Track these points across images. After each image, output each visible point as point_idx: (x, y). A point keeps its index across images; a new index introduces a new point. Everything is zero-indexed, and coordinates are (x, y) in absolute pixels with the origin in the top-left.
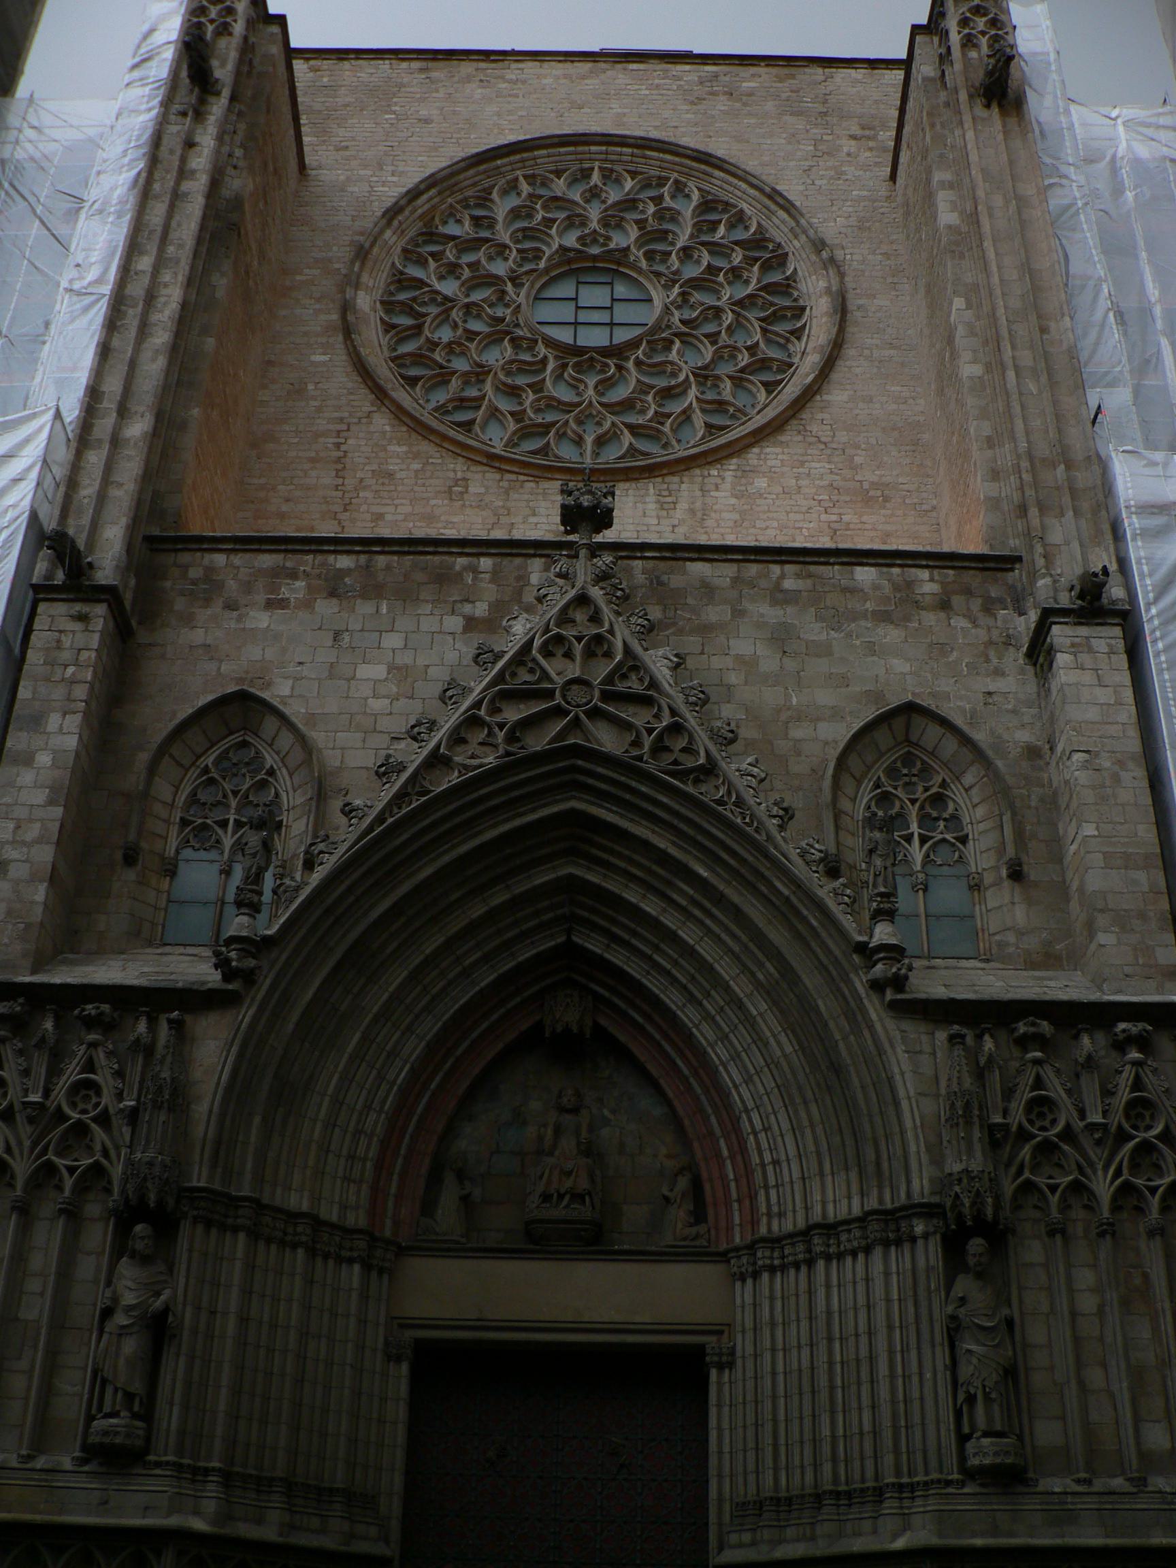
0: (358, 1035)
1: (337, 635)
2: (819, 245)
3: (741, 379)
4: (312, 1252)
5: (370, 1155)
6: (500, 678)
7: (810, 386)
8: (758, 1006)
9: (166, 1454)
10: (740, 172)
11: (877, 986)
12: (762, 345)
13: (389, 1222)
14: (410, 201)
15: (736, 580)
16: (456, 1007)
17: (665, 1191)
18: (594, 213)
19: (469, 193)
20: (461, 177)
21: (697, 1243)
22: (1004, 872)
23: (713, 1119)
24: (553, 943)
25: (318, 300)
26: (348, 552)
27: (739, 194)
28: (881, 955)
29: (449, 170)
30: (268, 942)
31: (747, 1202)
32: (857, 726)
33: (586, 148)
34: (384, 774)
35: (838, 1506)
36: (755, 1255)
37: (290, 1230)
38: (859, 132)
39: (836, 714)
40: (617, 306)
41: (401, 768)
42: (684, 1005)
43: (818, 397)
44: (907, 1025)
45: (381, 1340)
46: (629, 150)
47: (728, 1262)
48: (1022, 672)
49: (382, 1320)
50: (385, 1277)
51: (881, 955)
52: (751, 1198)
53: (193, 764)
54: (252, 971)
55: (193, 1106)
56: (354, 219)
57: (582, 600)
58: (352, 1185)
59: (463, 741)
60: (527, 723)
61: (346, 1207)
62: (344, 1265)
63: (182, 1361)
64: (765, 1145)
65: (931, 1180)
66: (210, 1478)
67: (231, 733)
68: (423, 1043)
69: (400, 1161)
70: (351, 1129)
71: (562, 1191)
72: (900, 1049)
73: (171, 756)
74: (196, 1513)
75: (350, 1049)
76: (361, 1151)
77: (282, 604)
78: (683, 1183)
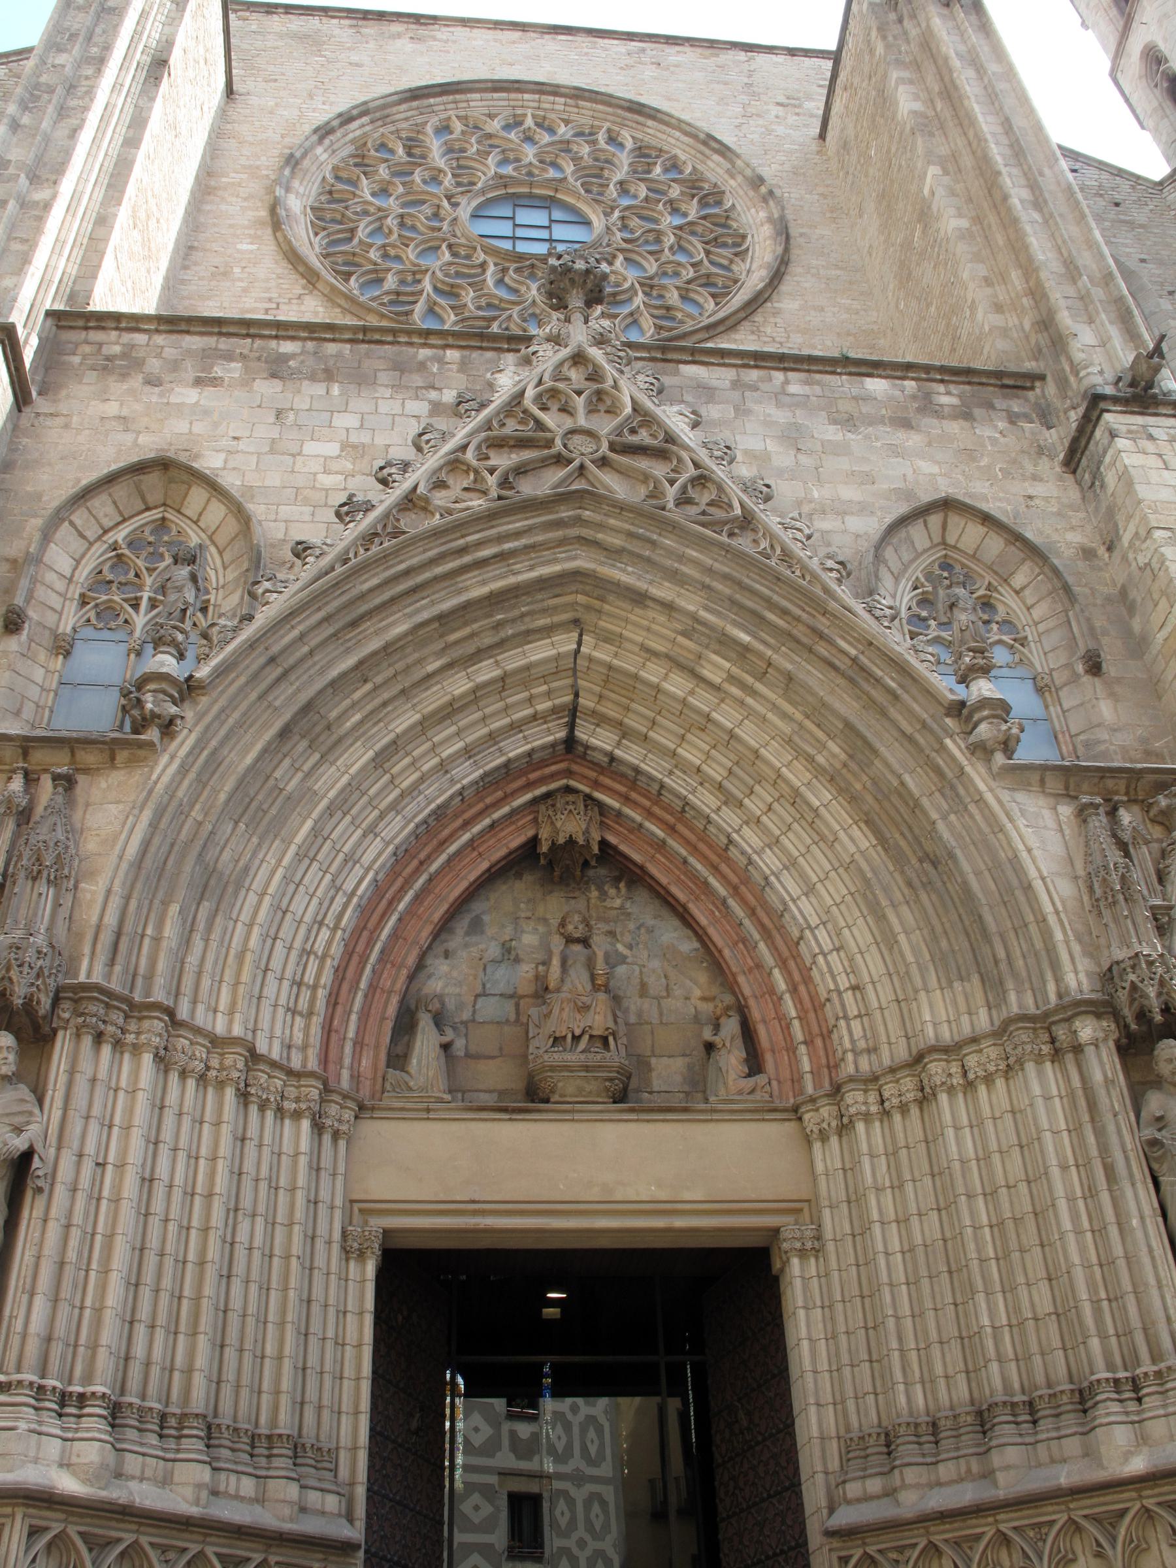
0: (309, 824)
1: (279, 414)
2: (757, 181)
3: (687, 290)
4: (244, 1096)
5: (322, 981)
6: (488, 425)
7: (760, 293)
8: (821, 796)
9: (19, 1370)
10: (673, 121)
11: (981, 750)
12: (706, 261)
13: (345, 1074)
14: (342, 124)
15: (736, 384)
16: (433, 806)
17: (707, 1035)
18: (529, 153)
19: (404, 125)
20: (394, 110)
21: (758, 1096)
22: (1080, 668)
23: (762, 945)
24: (551, 738)
25: (245, 199)
26: (293, 338)
27: (673, 141)
28: (986, 713)
29: (382, 101)
30: (189, 689)
31: (819, 1042)
32: (889, 519)
33: (520, 96)
34: (347, 514)
35: (1017, 1423)
36: (838, 1104)
37: (215, 1062)
38: (786, 101)
39: (863, 509)
40: (554, 226)
41: (368, 507)
42: (719, 809)
43: (769, 304)
44: (1020, 796)
45: (337, 1227)
46: (562, 100)
47: (800, 1119)
48: (1061, 479)
49: (338, 1202)
50: (342, 1144)
51: (986, 713)
52: (822, 1035)
53: (99, 538)
54: (171, 722)
55: (82, 885)
56: (283, 136)
57: (578, 358)
58: (298, 1019)
59: (440, 485)
60: (521, 470)
61: (289, 1047)
62: (287, 1122)
63: (54, 1230)
64: (838, 967)
65: (1088, 974)
66: (87, 1410)
67: (148, 509)
68: (391, 848)
69: (360, 996)
70: (297, 944)
71: (577, 1032)
72: (1021, 822)
73: (72, 523)
74: (65, 1464)
75: (299, 839)
76: (309, 978)
77: (215, 382)
78: (731, 1026)
